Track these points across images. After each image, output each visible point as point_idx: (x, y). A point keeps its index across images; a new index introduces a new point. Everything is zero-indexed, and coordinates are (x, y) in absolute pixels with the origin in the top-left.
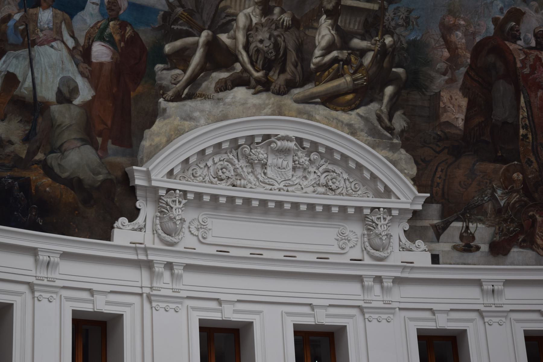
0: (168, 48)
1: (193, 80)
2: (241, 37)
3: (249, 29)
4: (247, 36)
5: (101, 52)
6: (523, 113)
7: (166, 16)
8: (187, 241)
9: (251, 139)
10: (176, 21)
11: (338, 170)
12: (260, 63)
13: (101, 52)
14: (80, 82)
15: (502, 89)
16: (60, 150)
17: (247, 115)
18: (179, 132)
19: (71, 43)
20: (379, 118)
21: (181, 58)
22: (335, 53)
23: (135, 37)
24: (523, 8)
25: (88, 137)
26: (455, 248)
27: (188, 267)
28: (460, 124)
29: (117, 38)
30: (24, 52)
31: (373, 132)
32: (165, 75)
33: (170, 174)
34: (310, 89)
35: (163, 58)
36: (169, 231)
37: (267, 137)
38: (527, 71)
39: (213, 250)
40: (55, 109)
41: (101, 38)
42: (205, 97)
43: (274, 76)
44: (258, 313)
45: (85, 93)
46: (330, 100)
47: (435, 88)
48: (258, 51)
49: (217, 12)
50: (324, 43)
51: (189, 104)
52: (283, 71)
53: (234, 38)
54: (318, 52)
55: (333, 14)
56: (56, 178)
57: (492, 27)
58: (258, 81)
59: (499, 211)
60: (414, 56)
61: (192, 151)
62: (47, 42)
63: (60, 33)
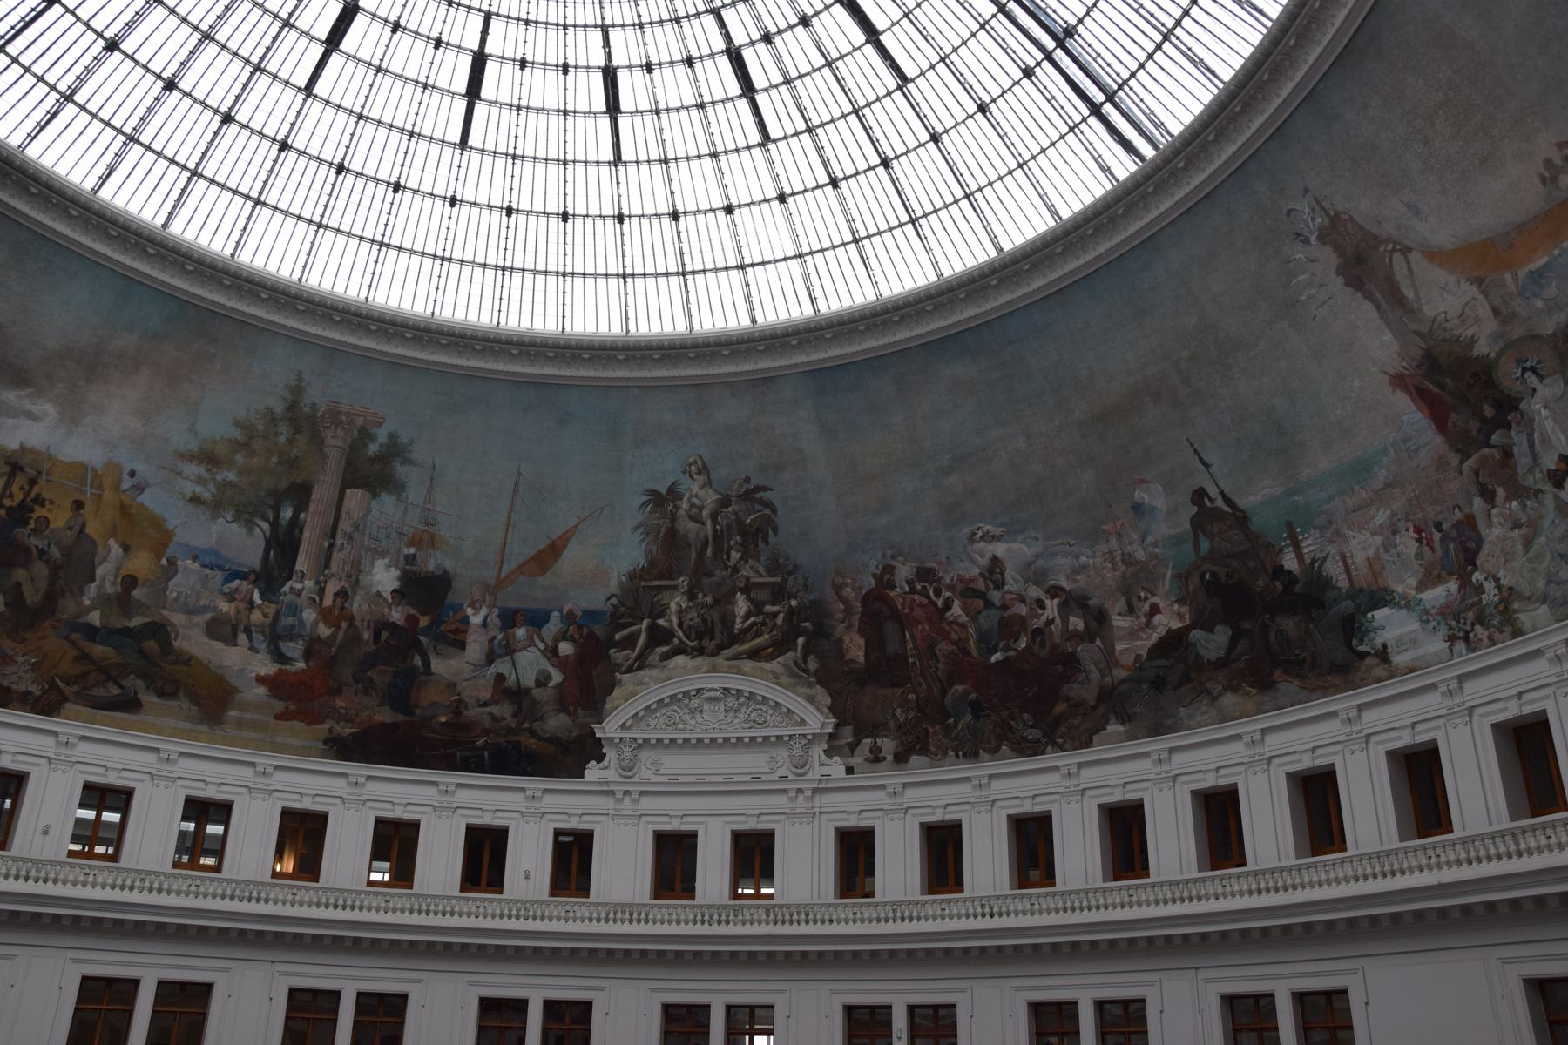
0: (617, 637)
1: (641, 656)
2: (675, 619)
3: (680, 612)
5: (565, 648)
6: (910, 645)
7: (612, 615)
9: (686, 694)
10: (621, 617)
12: (693, 636)
13: (565, 648)
14: (552, 671)
15: (890, 628)
16: (542, 719)
17: (687, 674)
18: (633, 694)
19: (542, 646)
20: (796, 663)
21: (630, 642)
23: (591, 635)
24: (893, 563)
25: (562, 705)
28: (862, 659)
31: (792, 674)
33: (623, 726)
34: (737, 648)
35: (615, 644)
36: (628, 769)
37: (698, 691)
39: (665, 779)
40: (535, 692)
41: (564, 639)
42: (652, 666)
45: (557, 677)
46: (754, 655)
50: (742, 612)
51: (640, 673)
52: (712, 638)
54: (738, 620)
55: (746, 590)
56: (540, 739)
58: (694, 649)
59: (899, 727)
62: (525, 648)
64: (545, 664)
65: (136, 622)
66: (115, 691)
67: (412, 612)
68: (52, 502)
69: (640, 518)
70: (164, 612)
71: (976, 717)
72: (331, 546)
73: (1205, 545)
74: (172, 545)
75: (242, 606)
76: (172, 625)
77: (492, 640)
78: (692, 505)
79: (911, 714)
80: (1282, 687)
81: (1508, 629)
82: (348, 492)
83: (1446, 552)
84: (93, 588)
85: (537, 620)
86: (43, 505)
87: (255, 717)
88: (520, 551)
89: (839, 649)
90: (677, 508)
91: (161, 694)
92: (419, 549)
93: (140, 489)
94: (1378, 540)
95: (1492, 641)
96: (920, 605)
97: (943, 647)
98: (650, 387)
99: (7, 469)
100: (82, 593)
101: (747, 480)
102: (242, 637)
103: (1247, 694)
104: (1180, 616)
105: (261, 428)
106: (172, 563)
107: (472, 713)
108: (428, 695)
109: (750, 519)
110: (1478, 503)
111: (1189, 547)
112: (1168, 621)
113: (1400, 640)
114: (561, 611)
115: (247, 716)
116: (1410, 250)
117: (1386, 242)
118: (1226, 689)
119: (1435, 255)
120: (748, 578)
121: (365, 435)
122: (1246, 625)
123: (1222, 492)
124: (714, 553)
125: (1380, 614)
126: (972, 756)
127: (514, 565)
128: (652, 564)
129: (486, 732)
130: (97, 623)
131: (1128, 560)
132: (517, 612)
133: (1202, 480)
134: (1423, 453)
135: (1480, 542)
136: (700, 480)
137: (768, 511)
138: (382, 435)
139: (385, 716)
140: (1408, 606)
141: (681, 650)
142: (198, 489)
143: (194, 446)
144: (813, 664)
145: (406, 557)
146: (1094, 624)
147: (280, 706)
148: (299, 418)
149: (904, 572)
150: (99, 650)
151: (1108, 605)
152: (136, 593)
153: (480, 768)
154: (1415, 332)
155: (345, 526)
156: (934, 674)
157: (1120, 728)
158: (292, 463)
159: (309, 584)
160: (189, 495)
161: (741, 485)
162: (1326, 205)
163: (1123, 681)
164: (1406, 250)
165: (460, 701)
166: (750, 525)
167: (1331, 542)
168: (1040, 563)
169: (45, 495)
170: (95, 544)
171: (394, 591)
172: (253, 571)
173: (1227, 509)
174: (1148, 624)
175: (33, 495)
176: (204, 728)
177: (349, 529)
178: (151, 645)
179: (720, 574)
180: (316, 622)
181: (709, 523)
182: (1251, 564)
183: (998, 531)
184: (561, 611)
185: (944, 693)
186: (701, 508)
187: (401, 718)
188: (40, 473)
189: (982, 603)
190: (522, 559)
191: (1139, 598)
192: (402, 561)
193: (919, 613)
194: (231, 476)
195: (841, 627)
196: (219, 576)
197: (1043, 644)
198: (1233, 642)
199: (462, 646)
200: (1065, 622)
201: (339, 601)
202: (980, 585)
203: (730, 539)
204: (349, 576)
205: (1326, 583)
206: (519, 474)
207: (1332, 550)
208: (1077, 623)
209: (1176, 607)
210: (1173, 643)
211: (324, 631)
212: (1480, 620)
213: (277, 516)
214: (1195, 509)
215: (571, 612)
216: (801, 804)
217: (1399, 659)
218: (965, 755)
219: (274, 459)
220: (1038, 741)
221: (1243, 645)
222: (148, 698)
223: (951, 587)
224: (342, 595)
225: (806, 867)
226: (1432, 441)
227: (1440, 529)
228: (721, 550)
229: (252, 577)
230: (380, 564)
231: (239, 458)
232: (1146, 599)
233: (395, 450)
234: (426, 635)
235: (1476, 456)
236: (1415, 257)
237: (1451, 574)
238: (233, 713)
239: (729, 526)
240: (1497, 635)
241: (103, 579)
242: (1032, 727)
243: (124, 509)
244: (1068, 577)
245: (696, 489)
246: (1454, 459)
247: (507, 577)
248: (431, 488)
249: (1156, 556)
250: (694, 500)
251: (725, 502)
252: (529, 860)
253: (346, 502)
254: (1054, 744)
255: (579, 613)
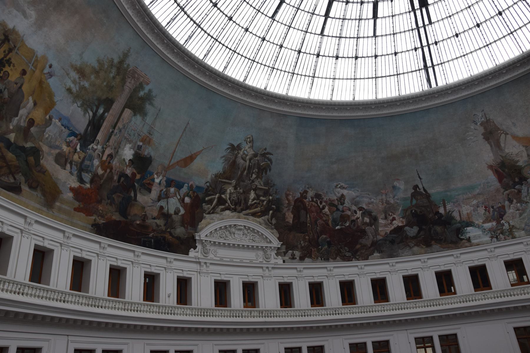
0: (207, 199)
1: (214, 208)
3: (231, 194)
4: (230, 196)
5: (187, 200)
6: (309, 219)
7: (206, 190)
8: (211, 256)
9: (230, 226)
10: (209, 191)
11: (256, 235)
12: (233, 204)
13: (187, 200)
15: (303, 212)
16: (174, 228)
17: (229, 218)
18: (209, 223)
19: (179, 197)
20: (268, 220)
21: (210, 202)
22: (255, 201)
23: (197, 196)
24: (308, 190)
25: (183, 223)
26: (290, 258)
27: (211, 264)
28: (291, 222)
29: (192, 196)
30: (166, 200)
31: (266, 224)
32: (205, 206)
33: (206, 236)
34: (248, 211)
36: (206, 253)
38: (309, 207)
39: (219, 259)
40: (174, 216)
41: (188, 196)
42: (217, 213)
43: (237, 207)
44: (232, 277)
45: (182, 211)
46: (254, 215)
47: (284, 212)
48: (233, 200)
49: (221, 189)
50: (252, 198)
51: (212, 215)
52: (240, 206)
53: (226, 196)
54: (250, 201)
55: (255, 190)
56: (173, 236)
57: (299, 195)
58: (233, 209)
59: (302, 247)
60: (278, 203)
61: (213, 229)
62: (172, 197)
63: (176, 194)
64: (179, 205)
65: (28, 145)
66: (12, 181)
67: (135, 171)
68: (14, 66)
69: (225, 154)
70: (41, 143)
71: (329, 247)
72: (113, 132)
73: (414, 202)
74: (53, 109)
75: (72, 150)
76: (42, 151)
77: (161, 191)
78: (244, 154)
79: (306, 243)
80: (434, 246)
81: (511, 236)
82: (126, 109)
83: (494, 214)
84: (15, 120)
85: (179, 186)
86: (10, 66)
87: (67, 208)
88: (180, 155)
89: (284, 218)
90: (238, 153)
91: (31, 187)
92: (143, 144)
93: (51, 75)
94: (472, 208)
95: (505, 239)
96: (314, 206)
97: (320, 222)
98: (245, 105)
99: (2, 37)
100: (10, 122)
101: (265, 149)
102: (68, 166)
103: (422, 247)
104: (402, 222)
105: (106, 66)
106: (51, 119)
107: (149, 221)
108: (135, 211)
109: (262, 164)
110: (507, 203)
111: (409, 202)
112: (398, 223)
113: (475, 236)
114: (188, 184)
115: (64, 206)
116: (508, 134)
117: (502, 130)
118: (415, 245)
119: (515, 137)
120: (257, 186)
121: (141, 87)
122: (424, 227)
123: (423, 188)
124: (247, 174)
125: (469, 229)
126: (327, 260)
127: (176, 161)
128: (224, 172)
129: (154, 231)
130: (12, 140)
131: (388, 202)
132: (172, 181)
133: (418, 182)
134: (492, 187)
135: (505, 213)
136: (249, 145)
137: (269, 162)
138: (147, 88)
139: (116, 217)
140: (479, 227)
141: (228, 209)
142: (72, 86)
143: (78, 64)
144: (274, 221)
145: (138, 146)
146: (373, 221)
147: (77, 204)
148: (121, 69)
149: (311, 194)
150: (10, 156)
151: (378, 216)
152: (33, 129)
153: (150, 246)
154: (501, 156)
155: (120, 125)
156: (315, 230)
157: (378, 255)
158: (110, 88)
159: (99, 147)
160: (68, 87)
161: (263, 151)
162: (487, 116)
163: (380, 240)
164: (506, 134)
165: (145, 215)
166: (262, 166)
167: (456, 207)
168: (358, 199)
169: (13, 60)
170: (23, 96)
171: (130, 160)
172: (80, 134)
173: (424, 192)
174: (391, 223)
175: (8, 58)
176: (45, 209)
177: (121, 127)
178: (31, 159)
179: (247, 182)
180: (98, 166)
181: (248, 161)
182: (429, 210)
183: (346, 186)
184: (188, 184)
185: (318, 237)
186: (247, 155)
187: (122, 219)
188: (15, 47)
189: (335, 209)
190: (179, 159)
191: (389, 215)
192: (136, 148)
193: (313, 209)
194: (87, 85)
195: (286, 209)
196: (66, 132)
197: (354, 225)
198: (419, 232)
199: (150, 191)
200: (363, 219)
201: (109, 158)
202: (336, 203)
203: (254, 169)
204: (115, 148)
205: (453, 218)
206: (188, 123)
207: (456, 209)
208: (367, 220)
209: (401, 219)
210: (399, 230)
211: (100, 172)
212: (502, 233)
213: (97, 111)
214: (413, 191)
215: (192, 186)
216: (267, 272)
217: (474, 241)
218: (324, 259)
219: (105, 84)
220: (350, 257)
221: (422, 233)
222: (25, 188)
223: (326, 202)
224: (111, 156)
225: (269, 297)
226: (497, 184)
227: (493, 207)
228: (250, 173)
229: (79, 137)
230: (128, 146)
231: (93, 77)
232: (391, 215)
233: (148, 98)
234: (138, 183)
235: (509, 191)
236: (509, 137)
237: (494, 220)
238: (58, 204)
239: (254, 164)
240: (507, 237)
241: (21, 117)
242: (348, 252)
243: (41, 83)
244: (366, 205)
245: (247, 148)
246: (502, 190)
247: (172, 165)
248: (156, 119)
249: (397, 203)
250: (245, 152)
251: (255, 155)
252: (168, 288)
253: (124, 114)
254: (355, 258)
255: (195, 186)
